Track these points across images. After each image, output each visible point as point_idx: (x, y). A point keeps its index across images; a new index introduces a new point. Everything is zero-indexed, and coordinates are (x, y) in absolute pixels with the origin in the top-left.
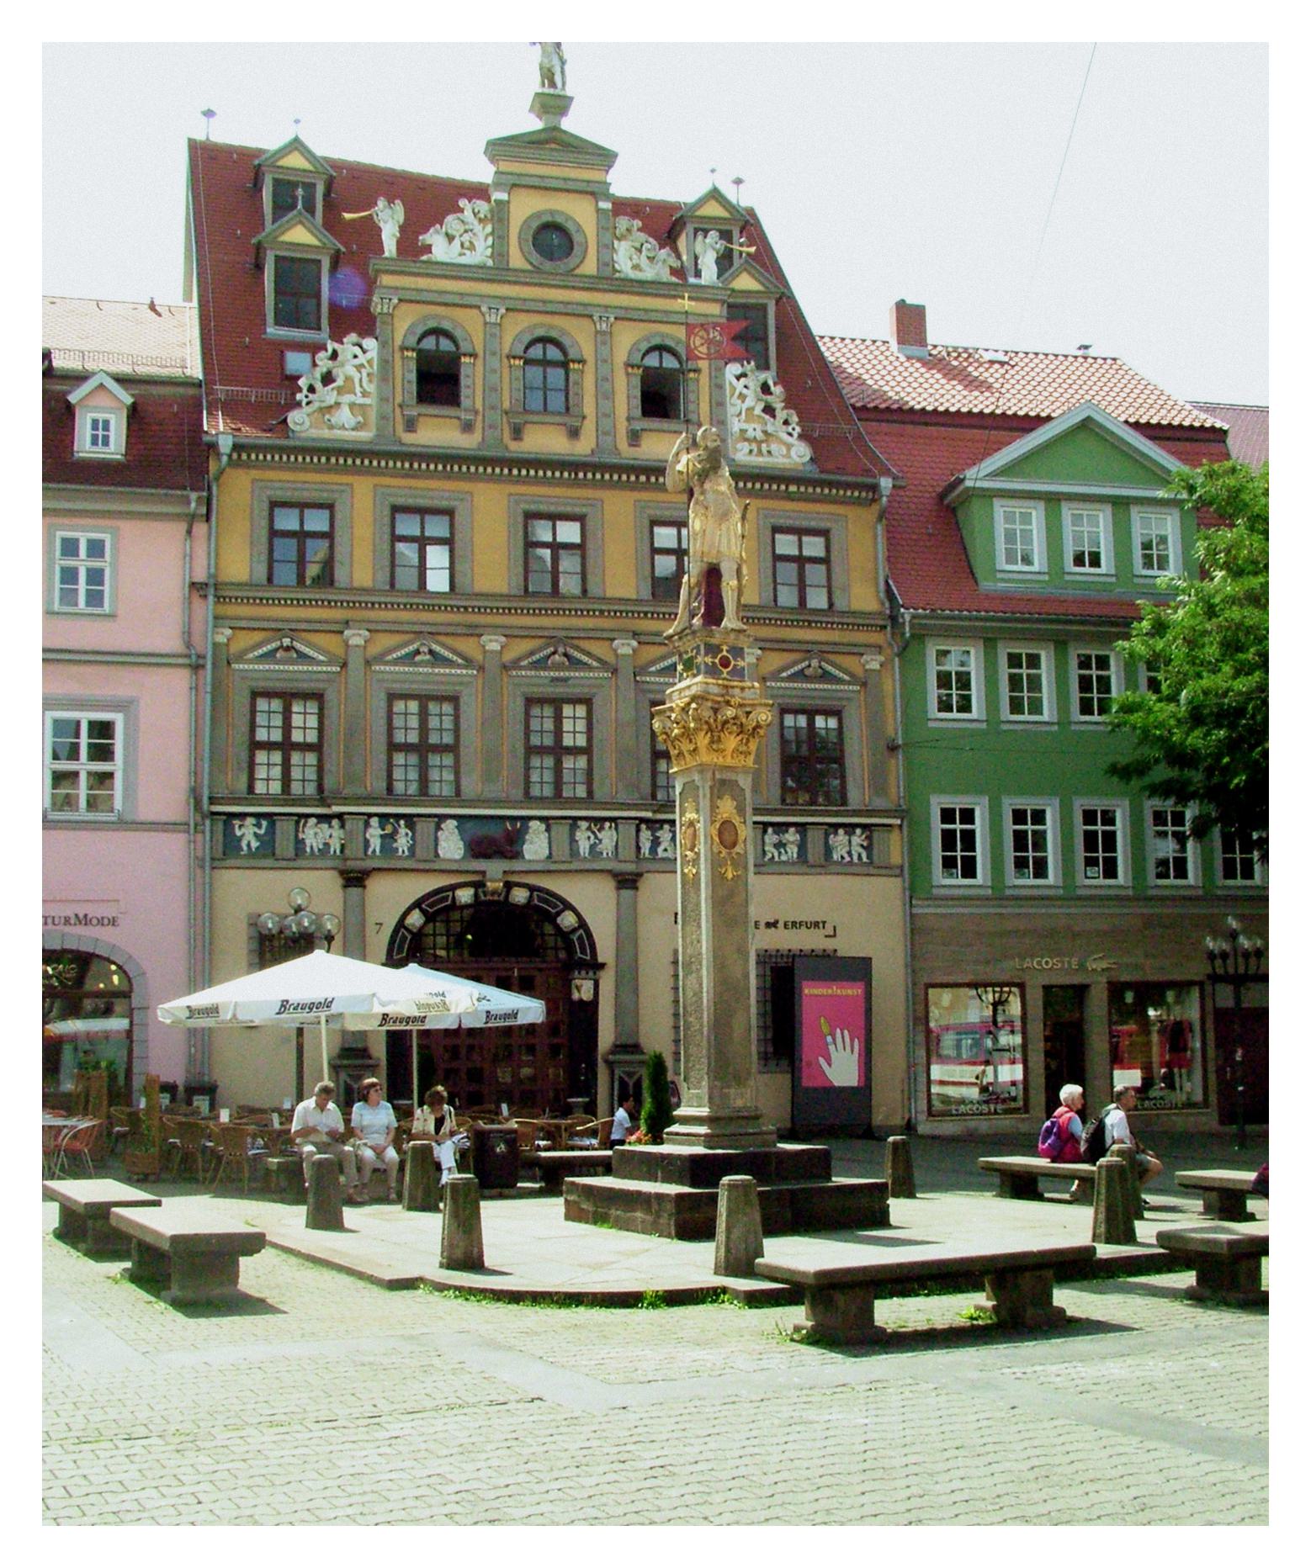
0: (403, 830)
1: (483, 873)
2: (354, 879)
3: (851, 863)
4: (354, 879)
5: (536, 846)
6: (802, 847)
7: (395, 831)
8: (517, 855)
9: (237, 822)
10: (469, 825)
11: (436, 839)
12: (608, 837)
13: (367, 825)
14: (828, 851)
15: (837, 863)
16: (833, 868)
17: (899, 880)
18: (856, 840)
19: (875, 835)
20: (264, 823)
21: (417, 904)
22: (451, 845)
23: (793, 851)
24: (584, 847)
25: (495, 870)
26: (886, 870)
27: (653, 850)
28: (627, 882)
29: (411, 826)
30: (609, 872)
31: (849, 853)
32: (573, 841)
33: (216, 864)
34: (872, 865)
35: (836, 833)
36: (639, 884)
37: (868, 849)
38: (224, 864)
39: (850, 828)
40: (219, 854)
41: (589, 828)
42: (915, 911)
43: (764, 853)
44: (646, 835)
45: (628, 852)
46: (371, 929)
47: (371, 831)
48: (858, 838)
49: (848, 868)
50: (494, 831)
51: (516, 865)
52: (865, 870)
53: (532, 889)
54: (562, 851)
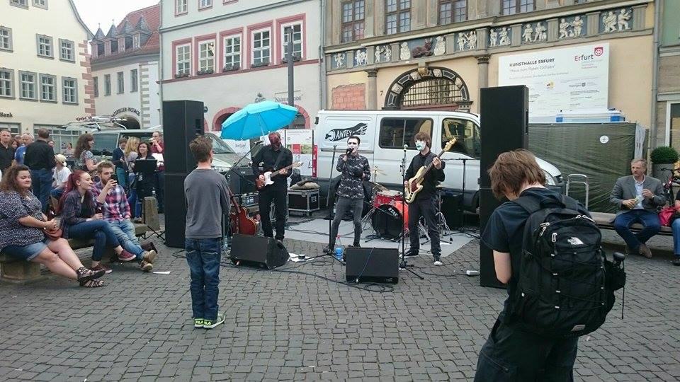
0: (387, 50)
1: (417, 64)
2: (373, 73)
3: (615, 32)
4: (373, 73)
5: (439, 49)
6: (584, 27)
7: (385, 51)
8: (431, 54)
9: (335, 56)
10: (413, 43)
11: (400, 52)
12: (472, 38)
13: (375, 50)
14: (601, 26)
15: (606, 33)
16: (603, 37)
17: (651, 37)
18: (621, 17)
19: (635, 11)
20: (344, 55)
21: (396, 81)
22: (406, 54)
23: (578, 30)
24: (461, 45)
25: (422, 62)
26: (642, 32)
27: (498, 42)
28: (484, 59)
29: (390, 48)
30: (476, 57)
31: (616, 26)
32: (456, 44)
33: (328, 73)
34: (633, 30)
35: (608, 16)
36: (490, 61)
37: (630, 20)
38: (332, 72)
39: (615, 10)
40: (329, 69)
41: (463, 36)
42: (661, 55)
43: (559, 34)
44: (493, 34)
45: (482, 45)
46: (379, 93)
47: (377, 52)
48: (623, 15)
49: (614, 35)
50: (421, 45)
51: (431, 59)
52: (625, 34)
53: (441, 69)
54: (450, 50)
